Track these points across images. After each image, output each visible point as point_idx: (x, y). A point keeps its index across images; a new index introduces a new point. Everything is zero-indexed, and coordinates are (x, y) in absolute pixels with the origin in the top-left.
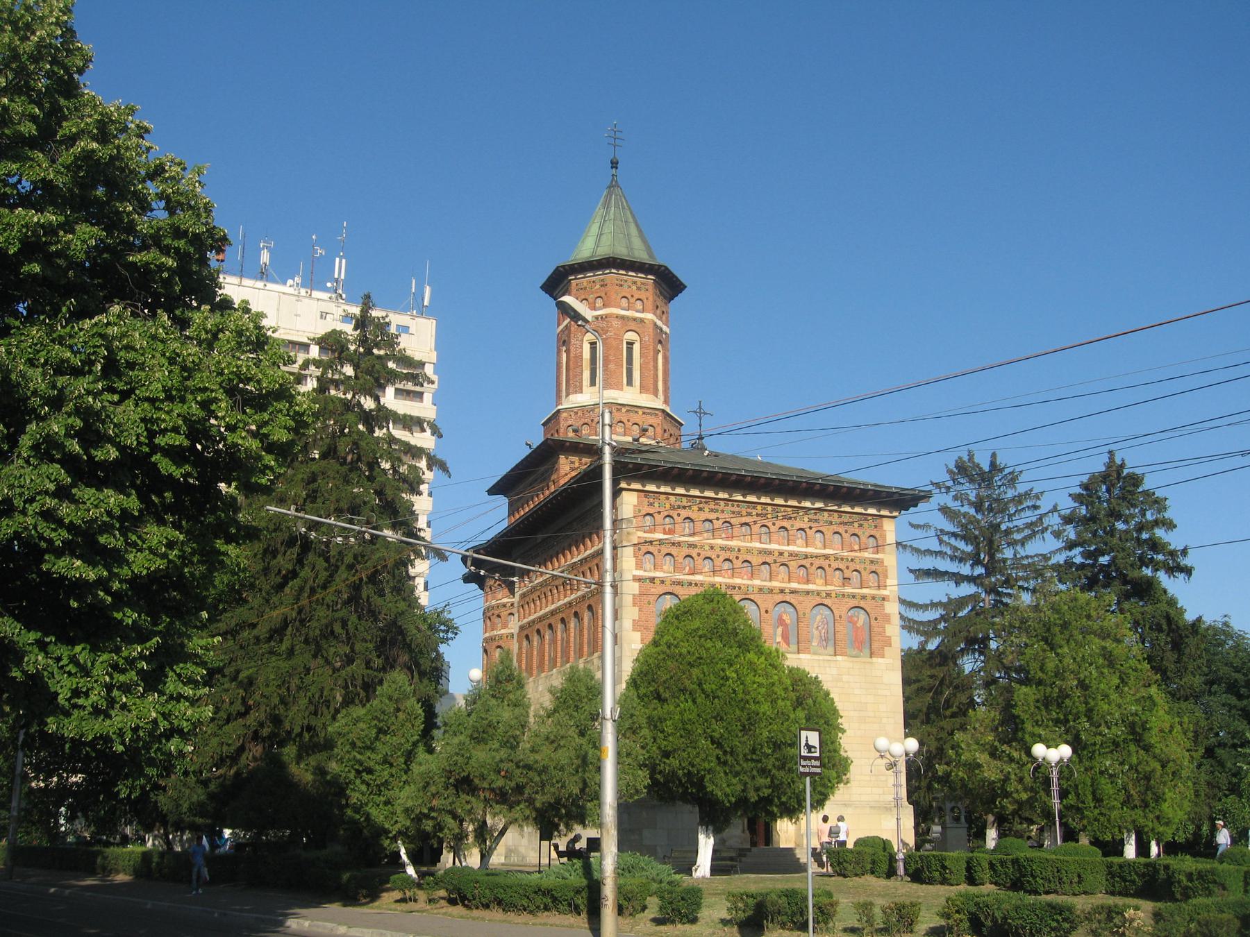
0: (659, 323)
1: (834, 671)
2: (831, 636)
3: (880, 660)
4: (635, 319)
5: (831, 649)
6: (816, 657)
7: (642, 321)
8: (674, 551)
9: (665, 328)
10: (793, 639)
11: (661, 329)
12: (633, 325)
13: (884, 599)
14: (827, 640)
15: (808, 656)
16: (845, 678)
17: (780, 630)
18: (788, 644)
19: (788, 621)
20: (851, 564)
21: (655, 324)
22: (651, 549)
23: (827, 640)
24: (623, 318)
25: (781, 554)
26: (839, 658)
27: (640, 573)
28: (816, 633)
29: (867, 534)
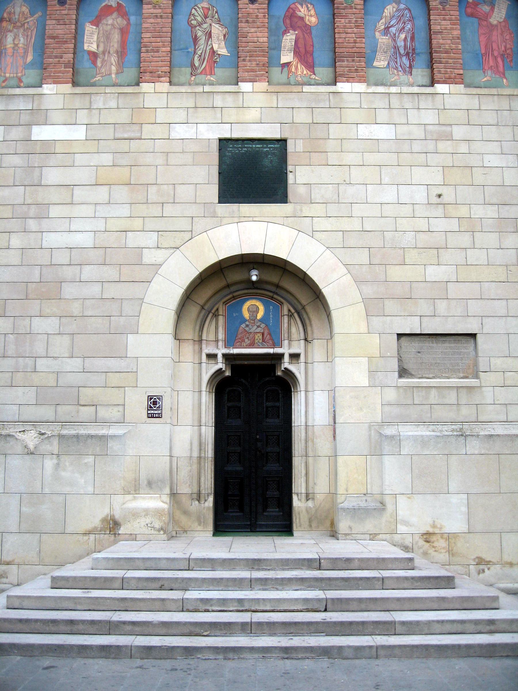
1: (430, 117)
2: (421, 46)
5: (420, 74)
6: (380, 89)
10: (321, 55)
14: (411, 54)
15: (360, 87)
16: (458, 132)
17: (289, 39)
18: (311, 67)
19: (312, 20)
23: (411, 54)
26: (441, 88)
28: (383, 40)
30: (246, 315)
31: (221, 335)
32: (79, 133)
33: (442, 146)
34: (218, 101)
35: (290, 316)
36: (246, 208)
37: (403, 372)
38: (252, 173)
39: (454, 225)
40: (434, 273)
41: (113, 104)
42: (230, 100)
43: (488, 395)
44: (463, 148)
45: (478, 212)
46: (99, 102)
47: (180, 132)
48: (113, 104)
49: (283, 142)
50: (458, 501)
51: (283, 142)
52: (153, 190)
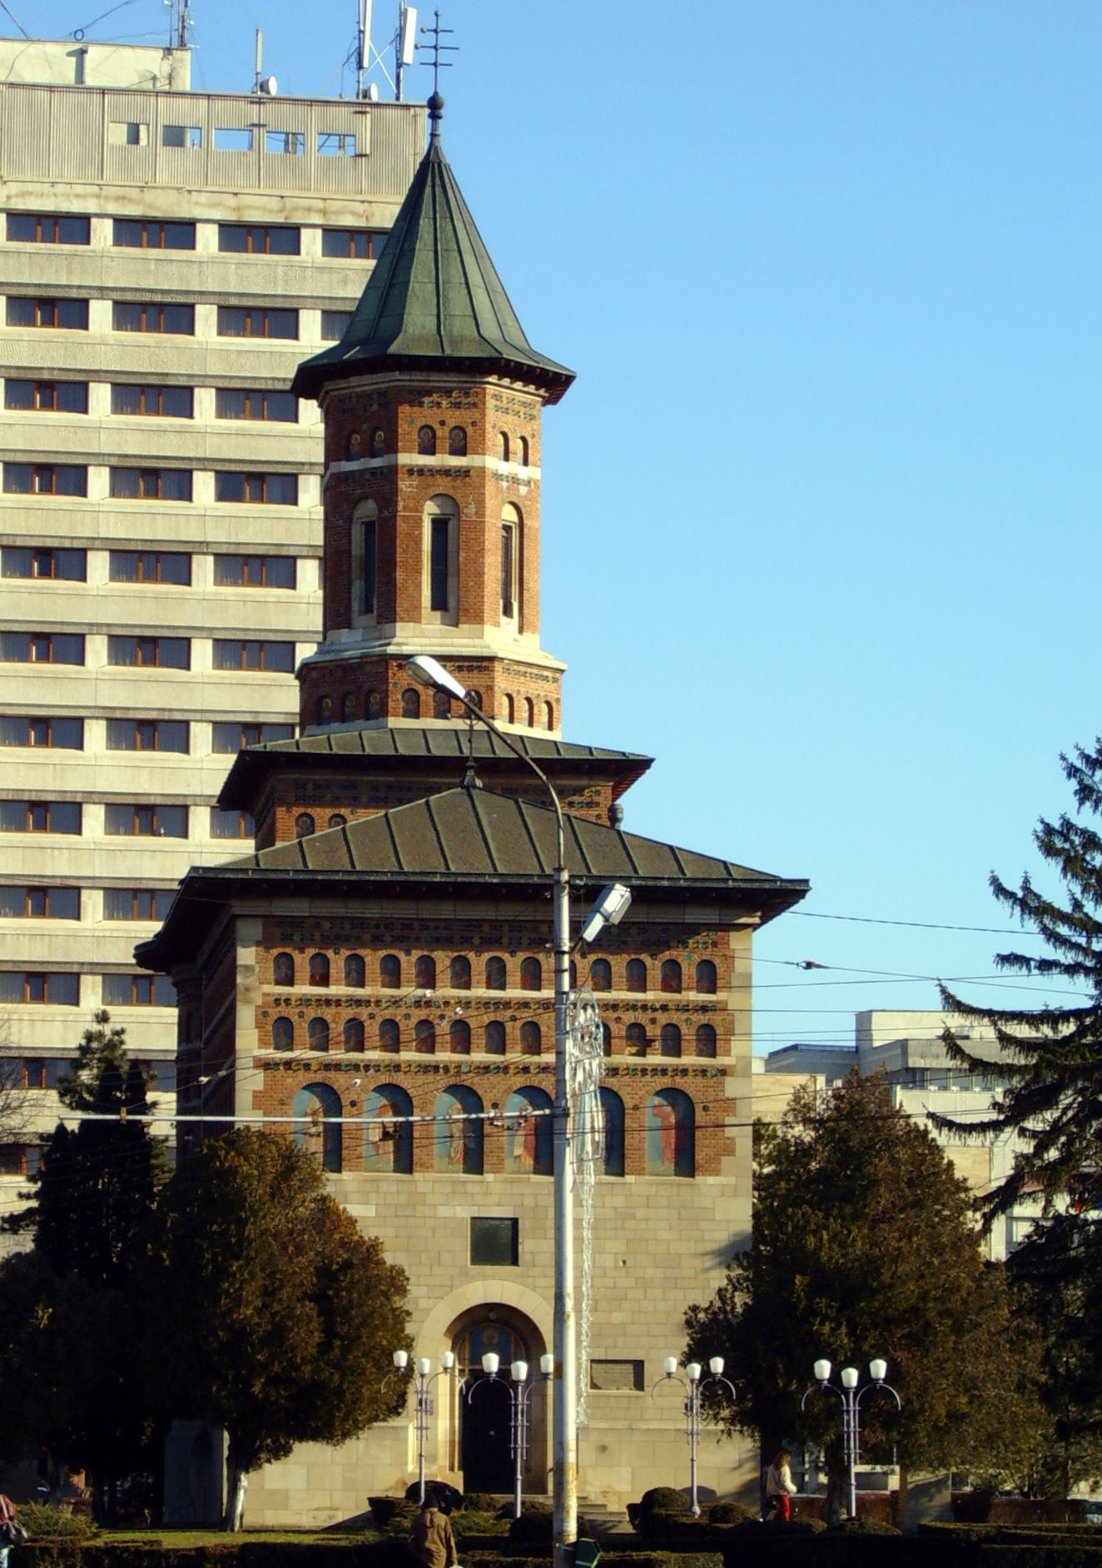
0: (505, 468)
1: (619, 1201)
3: (711, 1180)
4: (446, 472)
7: (465, 473)
8: (328, 1014)
9: (524, 473)
11: (515, 480)
12: (443, 485)
13: (723, 1072)
20: (659, 1015)
21: (498, 477)
22: (284, 1011)
24: (421, 471)
25: (525, 1004)
27: (270, 1053)
29: (697, 958)
30: (485, 1340)
31: (467, 1356)
32: (371, 1211)
33: (629, 1223)
34: (470, 1188)
35: (517, 1342)
36: (489, 1269)
37: (594, 1386)
38: (496, 1243)
39: (632, 1282)
40: (617, 1317)
41: (394, 1188)
42: (477, 1188)
43: (649, 1401)
44: (643, 1225)
45: (650, 1273)
46: (384, 1187)
47: (443, 1211)
48: (394, 1188)
49: (515, 1221)
50: (626, 1472)
51: (515, 1221)
52: (424, 1256)
